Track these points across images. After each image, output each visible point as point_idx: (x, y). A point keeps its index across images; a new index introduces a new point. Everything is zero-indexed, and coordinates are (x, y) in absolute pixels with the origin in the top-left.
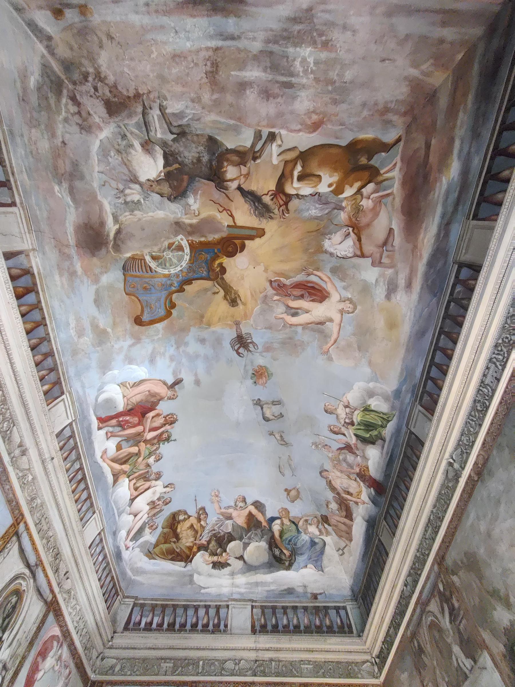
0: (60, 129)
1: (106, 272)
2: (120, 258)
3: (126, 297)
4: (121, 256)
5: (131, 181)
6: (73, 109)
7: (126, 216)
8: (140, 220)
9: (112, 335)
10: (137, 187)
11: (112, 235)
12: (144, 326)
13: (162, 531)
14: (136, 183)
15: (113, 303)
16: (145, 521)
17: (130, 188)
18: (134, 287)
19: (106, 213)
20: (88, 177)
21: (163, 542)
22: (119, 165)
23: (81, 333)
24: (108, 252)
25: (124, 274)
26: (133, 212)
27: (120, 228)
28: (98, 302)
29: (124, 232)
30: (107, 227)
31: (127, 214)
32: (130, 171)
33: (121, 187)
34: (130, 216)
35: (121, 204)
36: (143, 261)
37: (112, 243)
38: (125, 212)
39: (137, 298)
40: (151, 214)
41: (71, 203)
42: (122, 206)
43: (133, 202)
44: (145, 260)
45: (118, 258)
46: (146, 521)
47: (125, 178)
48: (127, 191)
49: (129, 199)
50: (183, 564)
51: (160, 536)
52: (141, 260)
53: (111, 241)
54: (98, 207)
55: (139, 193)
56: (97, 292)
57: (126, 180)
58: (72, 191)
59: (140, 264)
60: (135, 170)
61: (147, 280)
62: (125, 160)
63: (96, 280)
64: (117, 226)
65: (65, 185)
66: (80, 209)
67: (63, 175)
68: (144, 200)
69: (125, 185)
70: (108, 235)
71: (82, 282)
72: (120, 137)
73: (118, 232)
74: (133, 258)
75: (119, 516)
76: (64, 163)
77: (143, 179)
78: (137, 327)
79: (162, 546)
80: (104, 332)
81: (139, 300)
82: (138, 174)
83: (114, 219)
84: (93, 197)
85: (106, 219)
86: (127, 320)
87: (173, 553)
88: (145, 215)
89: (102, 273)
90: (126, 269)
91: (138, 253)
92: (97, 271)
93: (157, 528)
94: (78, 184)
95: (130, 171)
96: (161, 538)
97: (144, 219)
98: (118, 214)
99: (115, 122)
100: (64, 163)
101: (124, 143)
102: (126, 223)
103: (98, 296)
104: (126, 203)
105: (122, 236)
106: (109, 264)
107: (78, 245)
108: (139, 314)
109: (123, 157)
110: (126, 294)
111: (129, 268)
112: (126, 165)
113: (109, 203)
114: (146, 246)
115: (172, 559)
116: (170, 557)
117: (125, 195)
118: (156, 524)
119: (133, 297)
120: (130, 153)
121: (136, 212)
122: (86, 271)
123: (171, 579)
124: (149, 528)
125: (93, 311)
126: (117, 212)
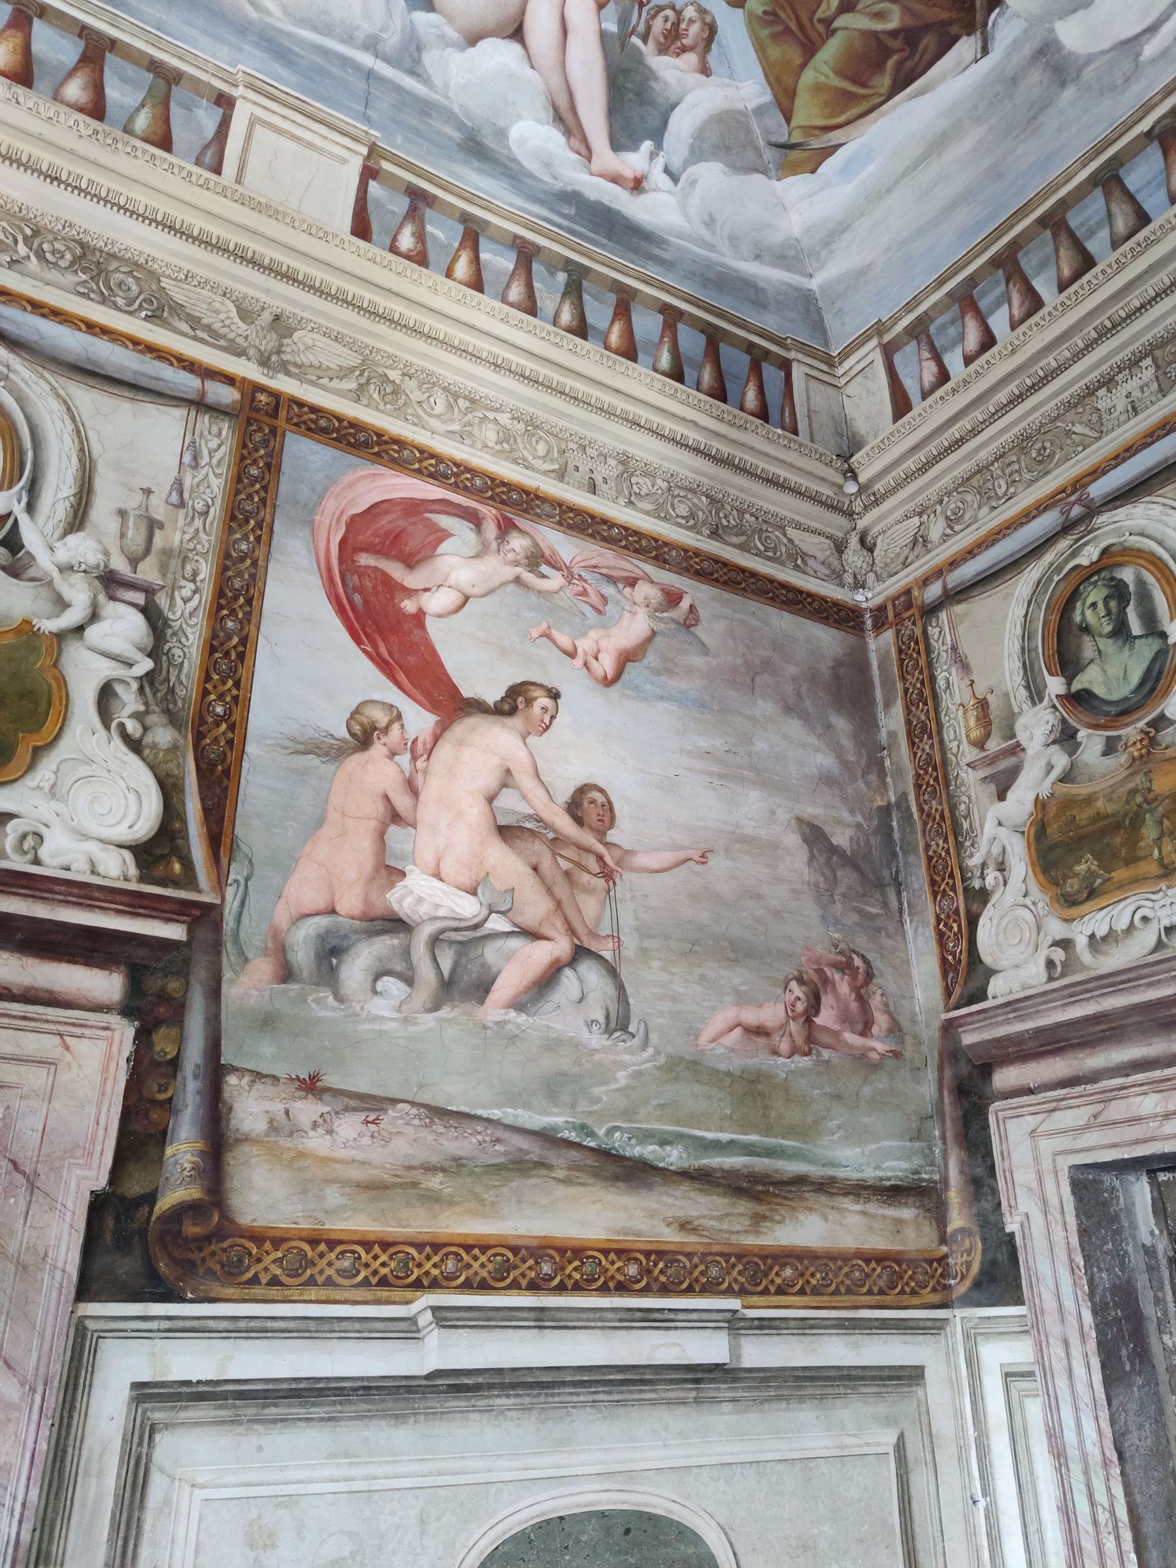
13: (751, 18)
16: (603, 36)
21: (797, 57)
46: (612, 27)
50: (966, 47)
51: (761, 50)
75: (412, 73)
79: (808, 77)
87: (884, 52)
93: (711, 30)
96: (775, 52)
115: (902, 81)
116: (884, 81)
118: (690, 12)
123: (960, 149)
124: (663, 50)
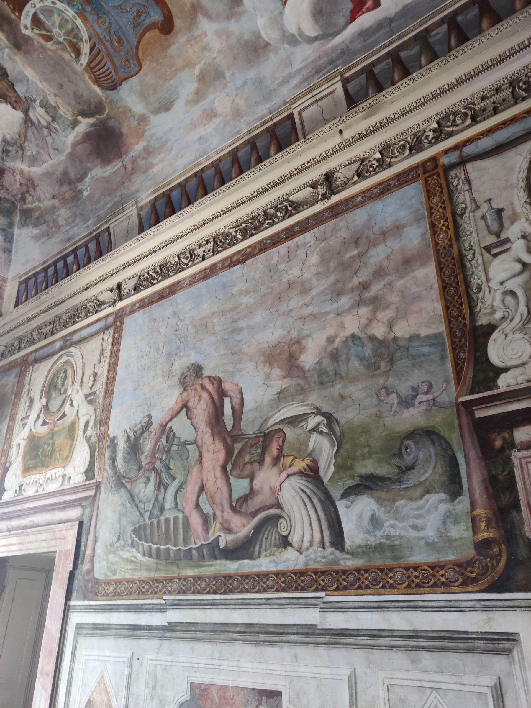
0: (48, 203)
1: (130, 110)
2: (107, 98)
3: (146, 65)
4: (104, 99)
5: (32, 124)
6: (29, 199)
7: (65, 113)
8: (56, 95)
9: (202, 63)
10: (31, 114)
11: (91, 120)
12: (169, 11)
14: (30, 119)
15: (161, 82)
17: (39, 122)
18: (128, 60)
19: (76, 137)
20: (61, 168)
22: (31, 143)
23: (210, 114)
24: (109, 117)
25: (120, 84)
26: (55, 108)
27: (79, 115)
28: (166, 106)
29: (80, 108)
30: (88, 130)
31: (62, 113)
32: (27, 130)
33: (46, 132)
34: (61, 108)
35: (58, 124)
36: (92, 65)
37: (98, 117)
38: (61, 116)
39: (137, 47)
40: (39, 84)
41: (89, 176)
42: (60, 122)
43: (47, 112)
44: (88, 64)
45: (108, 101)
47: (36, 132)
48: (44, 123)
49: (49, 119)
52: (92, 69)
53: (97, 118)
54: (78, 147)
55: (34, 109)
56: (156, 112)
57: (36, 129)
58: (81, 179)
59: (97, 68)
60: (20, 126)
61: (108, 45)
62: (23, 139)
63: (143, 119)
64: (80, 118)
65: (80, 186)
66: (89, 165)
67: (74, 191)
68: (35, 101)
69: (41, 128)
70: (93, 125)
71: (151, 136)
72: (9, 154)
73: (85, 114)
74: (97, 81)
76: (66, 192)
77: (19, 115)
78: (178, 23)
80: (202, 78)
81: (139, 42)
82: (21, 120)
83: (76, 126)
84: (72, 156)
85: (81, 134)
86: (173, 47)
88: (48, 92)
89: (133, 116)
90: (112, 84)
91: (86, 76)
92: (134, 122)
94: (72, 175)
95: (27, 130)
97: (51, 90)
98: (69, 123)
99: (4, 164)
100: (66, 192)
101: (10, 148)
102: (70, 110)
103: (159, 108)
104: (54, 119)
105: (85, 108)
106: (120, 110)
107: (119, 155)
108: (156, 32)
109: (22, 142)
110: (141, 67)
111: (110, 81)
112: (26, 136)
113: (66, 137)
114: (74, 72)
117: (49, 124)
119: (140, 55)
120: (12, 138)
121: (53, 104)
122: (140, 136)
125: (179, 106)
126: (68, 125)
